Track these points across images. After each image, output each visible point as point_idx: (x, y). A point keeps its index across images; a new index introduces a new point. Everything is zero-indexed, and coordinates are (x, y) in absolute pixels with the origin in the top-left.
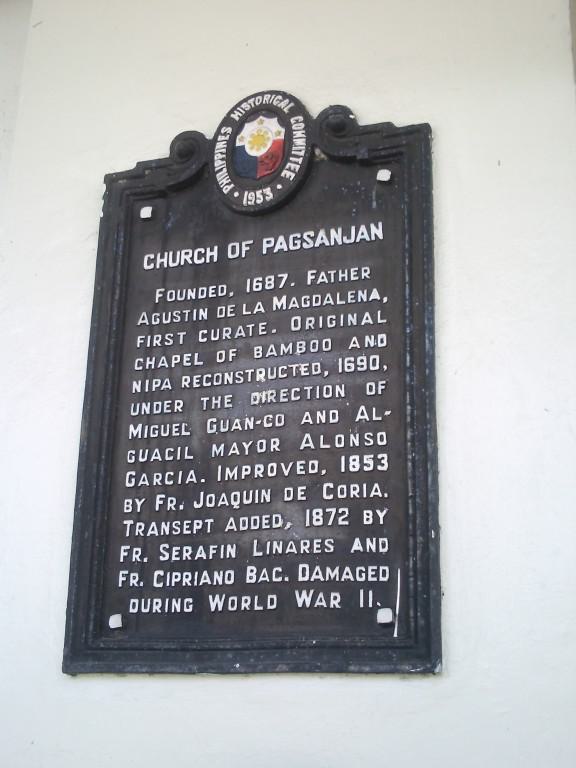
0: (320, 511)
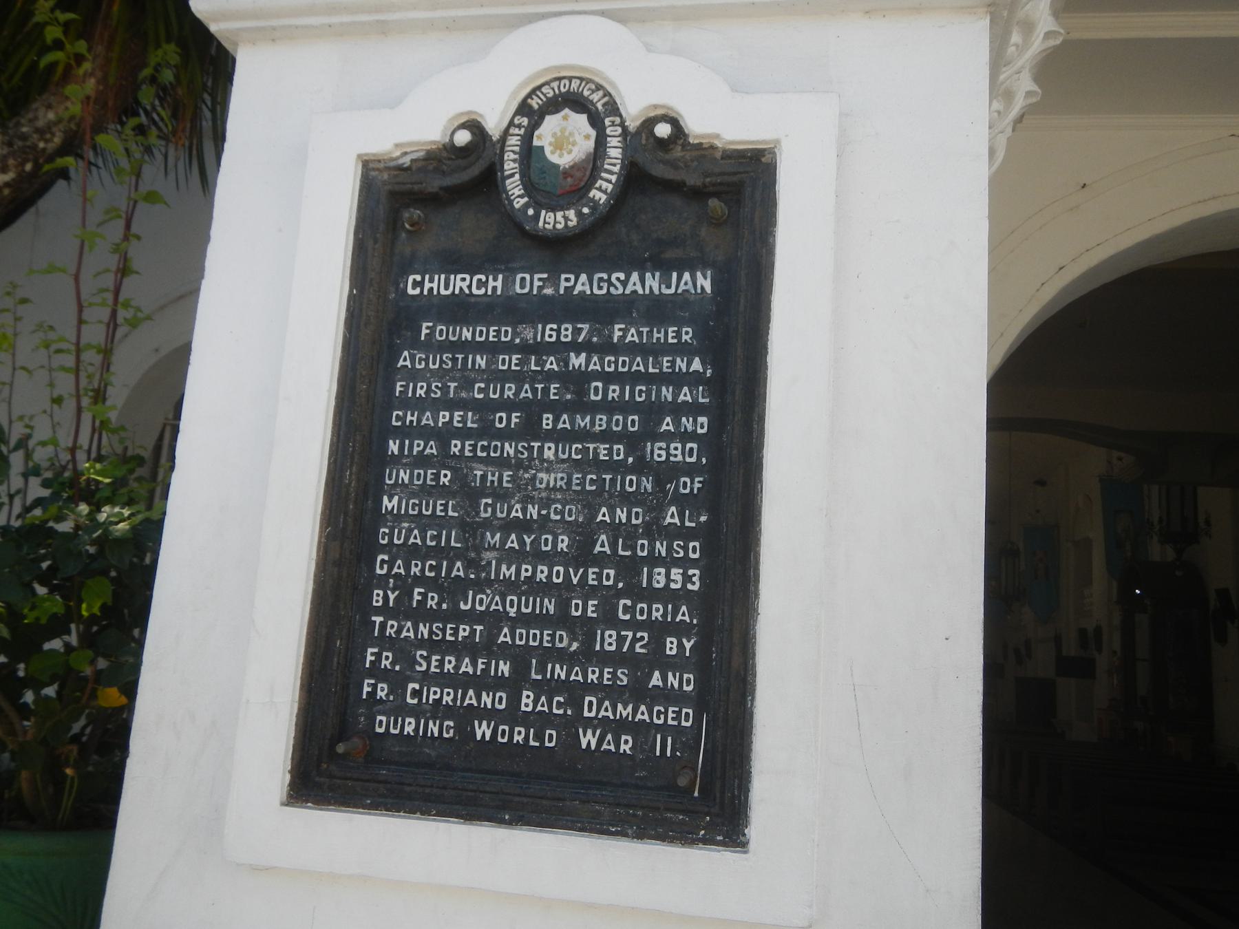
0: (614, 633)
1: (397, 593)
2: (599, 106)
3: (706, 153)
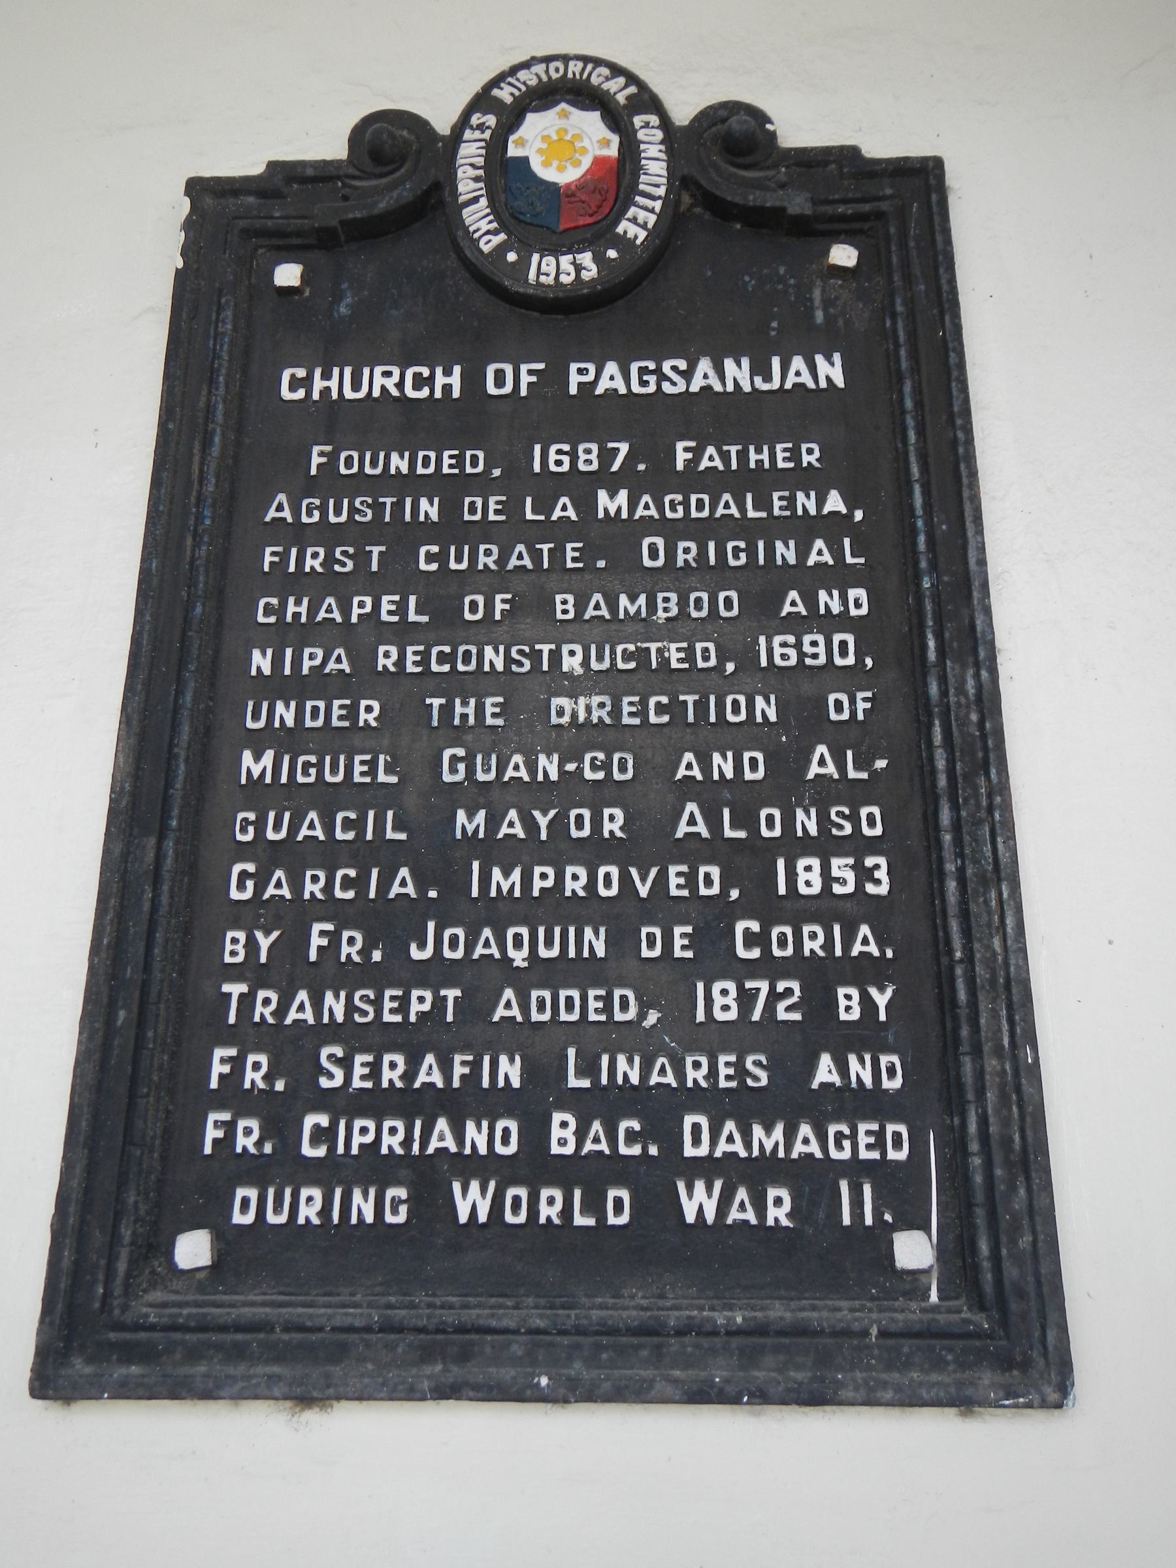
0: (731, 986)
1: (275, 934)
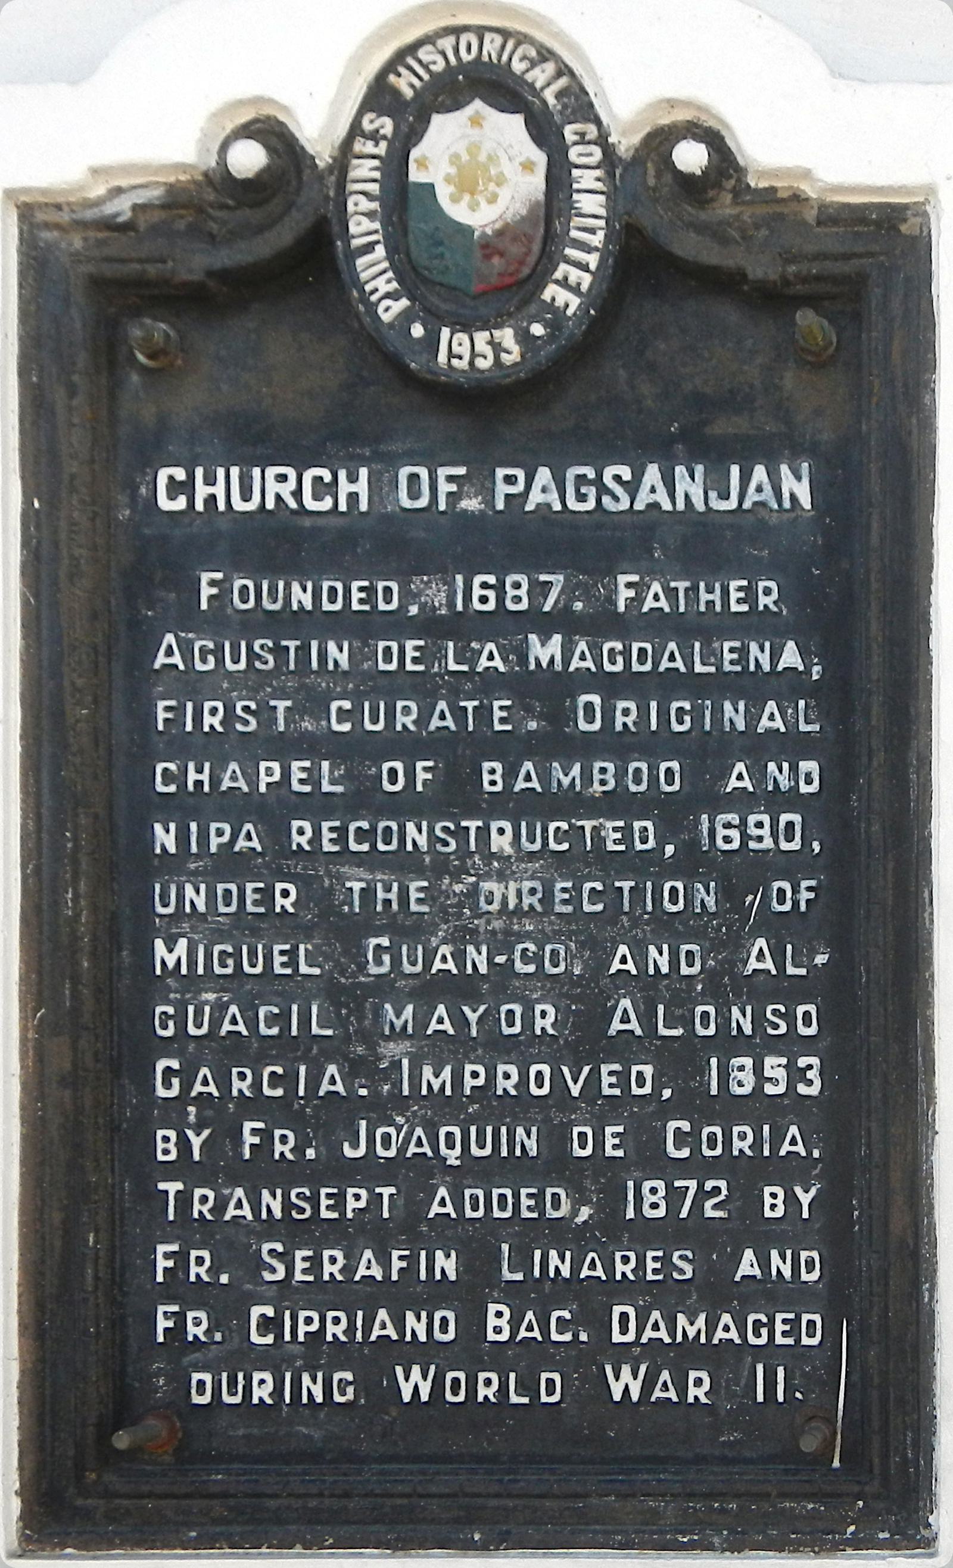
0: (660, 1184)
1: (206, 1133)
2: (549, 96)
3: (786, 211)
